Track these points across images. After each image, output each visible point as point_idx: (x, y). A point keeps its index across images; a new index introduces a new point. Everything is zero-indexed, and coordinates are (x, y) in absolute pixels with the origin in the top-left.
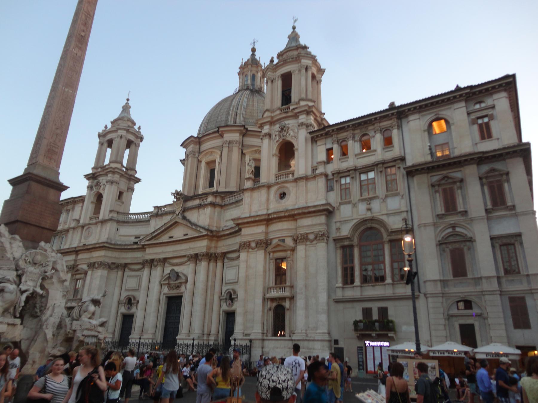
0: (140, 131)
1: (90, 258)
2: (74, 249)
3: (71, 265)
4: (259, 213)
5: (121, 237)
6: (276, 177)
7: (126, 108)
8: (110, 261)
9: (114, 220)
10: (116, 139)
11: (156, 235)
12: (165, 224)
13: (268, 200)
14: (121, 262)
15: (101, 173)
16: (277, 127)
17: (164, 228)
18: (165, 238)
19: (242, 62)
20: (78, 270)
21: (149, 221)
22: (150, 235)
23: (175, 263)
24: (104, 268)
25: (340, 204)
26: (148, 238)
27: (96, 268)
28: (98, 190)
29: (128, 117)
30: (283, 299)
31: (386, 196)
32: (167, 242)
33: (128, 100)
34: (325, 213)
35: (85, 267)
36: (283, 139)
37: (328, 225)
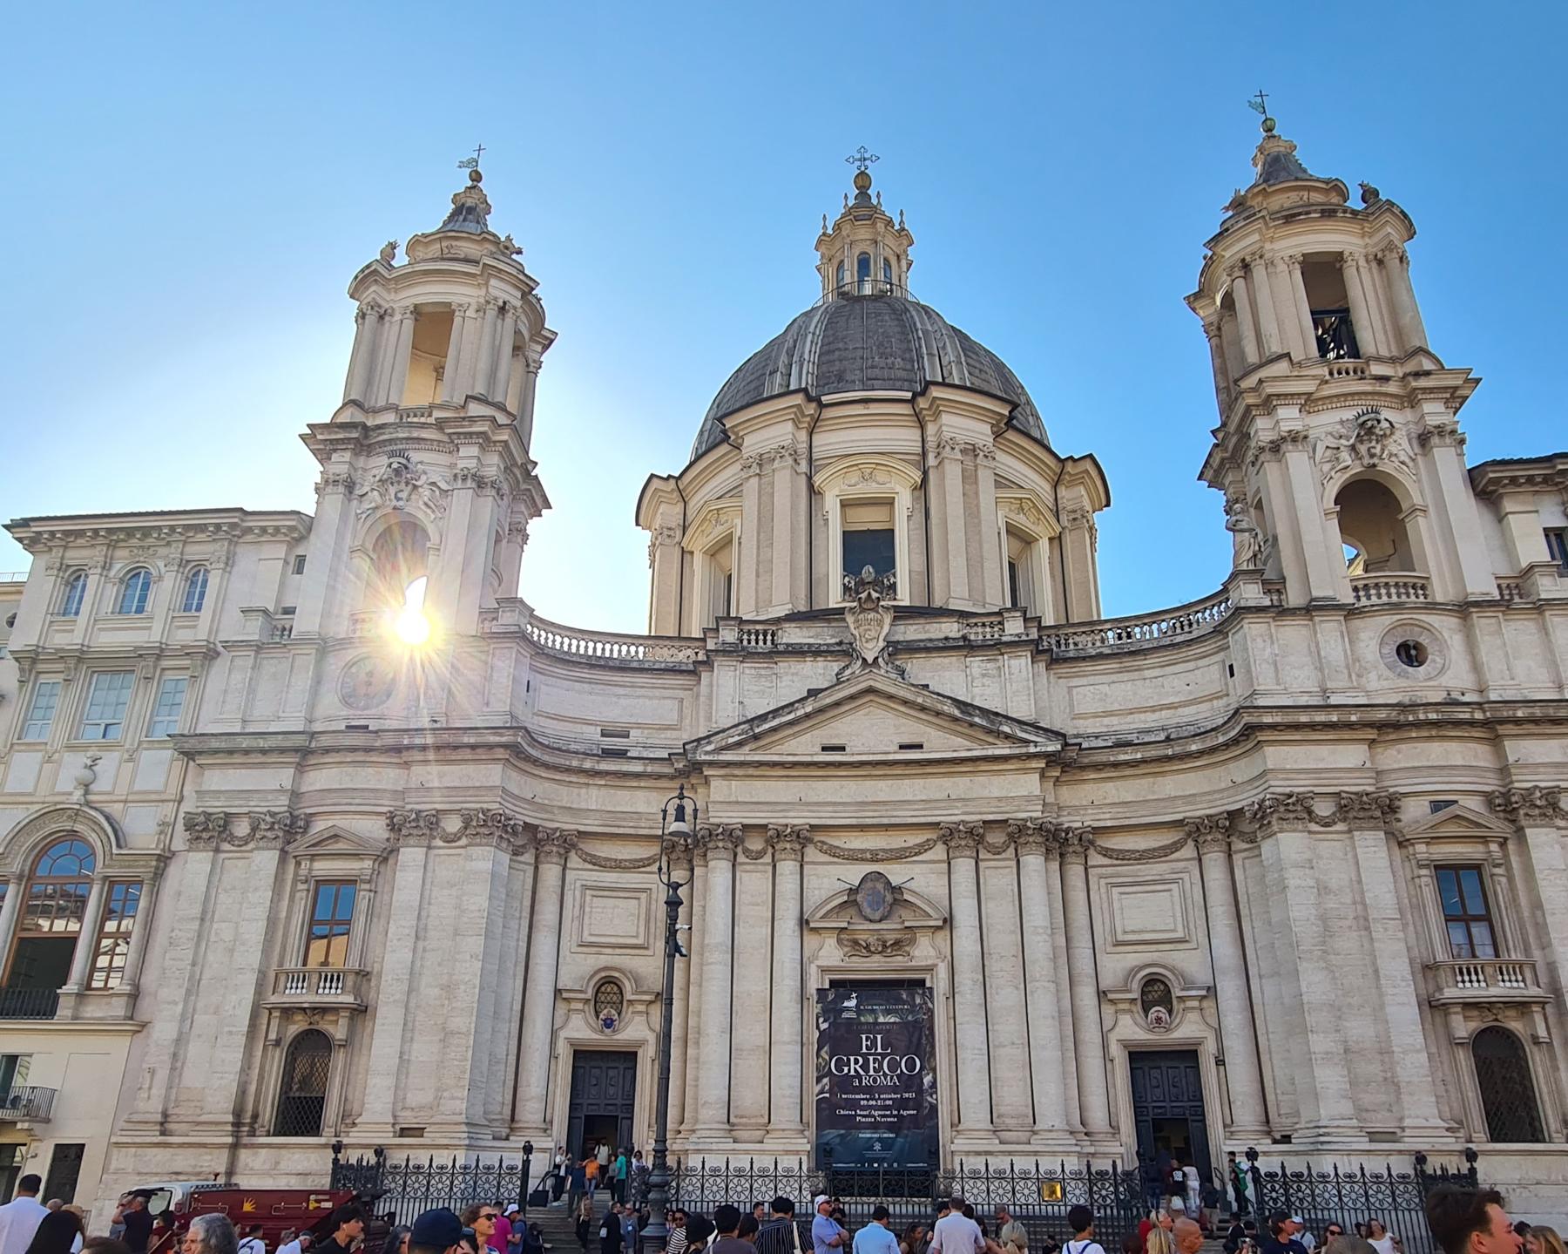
1: (401, 794)
2: (299, 741)
3: (273, 815)
4: (1334, 700)
6: (1356, 589)
10: (471, 313)
11: (756, 729)
12: (813, 693)
14: (557, 825)
16: (1329, 423)
17: (809, 709)
18: (804, 746)
22: (746, 727)
23: (863, 851)
26: (731, 740)
27: (450, 839)
28: (401, 503)
30: (1522, 1007)
35: (374, 829)
36: (1374, 465)
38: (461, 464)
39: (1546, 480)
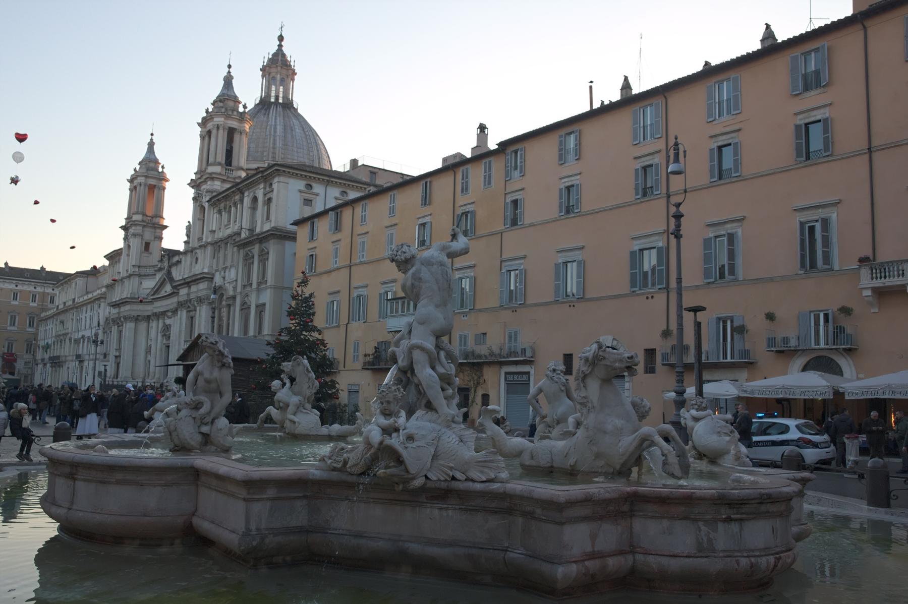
0: (164, 170)
5: (145, 290)
7: (151, 145)
8: (135, 314)
9: (136, 275)
13: (191, 264)
15: (128, 226)
19: (264, 62)
20: (118, 323)
21: (155, 275)
24: (130, 321)
25: (217, 271)
29: (152, 157)
31: (231, 266)
32: (163, 297)
33: (152, 135)
34: (206, 279)
37: (208, 288)
38: (133, 231)
39: (215, 204)
